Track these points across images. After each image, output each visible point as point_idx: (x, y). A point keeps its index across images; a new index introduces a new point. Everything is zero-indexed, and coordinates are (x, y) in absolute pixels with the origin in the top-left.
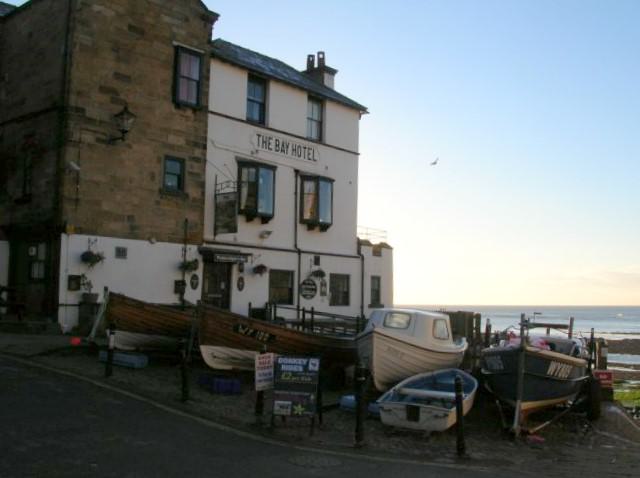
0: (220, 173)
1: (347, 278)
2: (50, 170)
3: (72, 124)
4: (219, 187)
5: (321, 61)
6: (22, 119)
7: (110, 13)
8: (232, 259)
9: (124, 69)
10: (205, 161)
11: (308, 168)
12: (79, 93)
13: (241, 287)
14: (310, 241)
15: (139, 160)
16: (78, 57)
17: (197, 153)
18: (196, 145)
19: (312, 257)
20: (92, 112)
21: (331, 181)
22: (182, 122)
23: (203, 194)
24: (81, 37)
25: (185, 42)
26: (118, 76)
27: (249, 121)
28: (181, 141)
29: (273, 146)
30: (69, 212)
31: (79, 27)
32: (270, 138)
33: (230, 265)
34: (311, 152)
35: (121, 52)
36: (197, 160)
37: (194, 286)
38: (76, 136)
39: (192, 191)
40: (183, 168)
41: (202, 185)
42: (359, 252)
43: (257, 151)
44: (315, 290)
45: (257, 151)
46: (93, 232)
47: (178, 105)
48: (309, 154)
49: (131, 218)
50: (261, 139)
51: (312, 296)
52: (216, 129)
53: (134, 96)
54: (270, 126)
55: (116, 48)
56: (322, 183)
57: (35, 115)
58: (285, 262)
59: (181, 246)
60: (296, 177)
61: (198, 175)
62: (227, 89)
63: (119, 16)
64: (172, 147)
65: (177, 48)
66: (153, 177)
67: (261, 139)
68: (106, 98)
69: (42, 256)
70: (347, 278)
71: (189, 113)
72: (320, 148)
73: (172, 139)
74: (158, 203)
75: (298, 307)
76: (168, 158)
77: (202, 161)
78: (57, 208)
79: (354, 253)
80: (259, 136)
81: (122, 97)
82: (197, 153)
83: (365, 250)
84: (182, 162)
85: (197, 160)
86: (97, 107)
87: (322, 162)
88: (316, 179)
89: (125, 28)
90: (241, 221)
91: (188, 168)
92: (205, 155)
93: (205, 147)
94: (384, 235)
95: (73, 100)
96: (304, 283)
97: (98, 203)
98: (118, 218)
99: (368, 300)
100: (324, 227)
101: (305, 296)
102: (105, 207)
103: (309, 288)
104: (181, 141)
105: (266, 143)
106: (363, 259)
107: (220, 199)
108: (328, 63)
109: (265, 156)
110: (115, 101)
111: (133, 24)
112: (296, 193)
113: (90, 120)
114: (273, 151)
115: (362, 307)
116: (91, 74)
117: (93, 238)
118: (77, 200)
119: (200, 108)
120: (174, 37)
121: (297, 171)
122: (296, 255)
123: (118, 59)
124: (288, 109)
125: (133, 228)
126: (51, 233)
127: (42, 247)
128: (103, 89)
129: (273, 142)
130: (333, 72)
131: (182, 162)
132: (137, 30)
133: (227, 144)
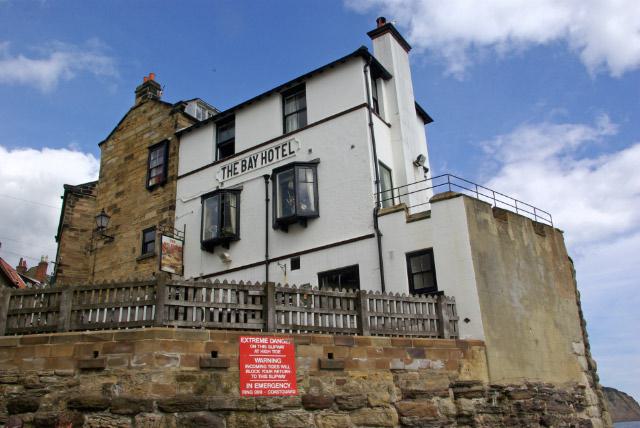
9: (121, 188)
14: (283, 245)
17: (165, 215)
18: (164, 210)
19: (288, 262)
22: (157, 200)
28: (154, 214)
29: (239, 167)
34: (286, 148)
43: (222, 183)
45: (222, 183)
47: (151, 189)
48: (283, 150)
50: (226, 171)
60: (267, 183)
66: (134, 250)
67: (226, 171)
71: (160, 190)
74: (136, 268)
82: (165, 215)
87: (302, 146)
93: (173, 208)
104: (154, 214)
106: (380, 235)
112: (267, 200)
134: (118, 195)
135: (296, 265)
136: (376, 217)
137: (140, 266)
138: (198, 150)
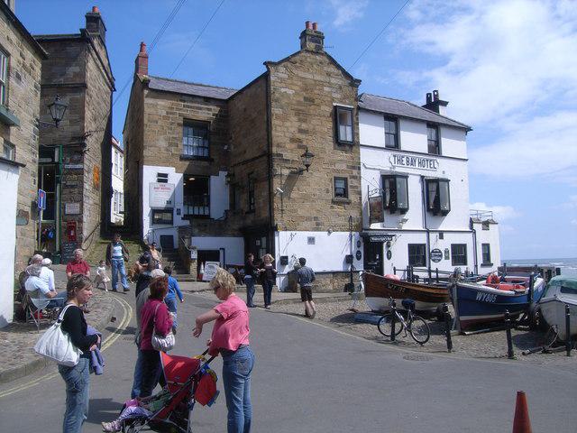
0: (370, 185)
1: (465, 246)
2: (265, 194)
3: (275, 164)
4: (370, 193)
5: (436, 97)
6: (246, 162)
7: (290, 92)
8: (383, 239)
9: (304, 126)
10: (360, 177)
11: (431, 174)
12: (278, 146)
13: (389, 258)
15: (317, 182)
16: (275, 122)
17: (355, 172)
18: (354, 168)
20: (287, 155)
21: (448, 181)
22: (342, 155)
23: (361, 200)
24: (276, 110)
25: (341, 102)
26: (301, 131)
27: (388, 148)
28: (344, 167)
29: (405, 162)
30: (278, 221)
31: (273, 104)
32: (403, 157)
33: (382, 243)
35: (302, 115)
36: (354, 177)
37: (359, 258)
38: (279, 172)
39: (352, 197)
40: (346, 184)
41: (360, 193)
42: (471, 227)
44: (441, 256)
45: (394, 167)
46: (295, 230)
47: (338, 143)
49: (316, 218)
51: (439, 260)
52: (366, 157)
53: (313, 144)
54: (402, 149)
55: (298, 113)
56: (441, 183)
57: (254, 159)
58: (420, 239)
59: (348, 233)
61: (356, 187)
62: (371, 132)
63: (296, 93)
64: (338, 171)
65: (335, 107)
66: (328, 192)
68: (294, 146)
69: (264, 245)
70: (465, 246)
72: (439, 160)
73: (338, 166)
75: (430, 268)
76: (336, 179)
77: (358, 178)
78: (271, 217)
79: (468, 230)
80: (395, 156)
81: (304, 143)
82: (355, 172)
83: (477, 227)
84: (346, 179)
85: (354, 177)
86: (292, 154)
87: (441, 169)
88: (437, 181)
89: (302, 100)
90: (387, 216)
91: (349, 184)
92: (359, 173)
93: (359, 169)
94: (490, 214)
95: (275, 150)
96: (433, 252)
97: (296, 211)
98: (308, 219)
99: (480, 261)
100: (445, 213)
101: (434, 261)
102: (300, 212)
103: (437, 255)
104: (344, 167)
105: (400, 161)
107: (372, 201)
108: (441, 98)
109: (399, 170)
110: (300, 147)
111: (307, 96)
112: (423, 192)
113: (287, 161)
114: (406, 165)
115: (476, 266)
116: (283, 131)
117: (294, 232)
118: (282, 210)
119: (353, 145)
120: (333, 100)
121: (422, 177)
122: (425, 235)
123: (299, 120)
124: (414, 140)
125: (318, 224)
126: (269, 230)
127: (264, 240)
128: (293, 140)
129: (404, 159)
130: (445, 104)
131: (346, 179)
132: (310, 100)
133: (374, 164)
134: (301, 131)
135: (441, 237)
136: (472, 222)
137: (335, 206)
138: (371, 132)
